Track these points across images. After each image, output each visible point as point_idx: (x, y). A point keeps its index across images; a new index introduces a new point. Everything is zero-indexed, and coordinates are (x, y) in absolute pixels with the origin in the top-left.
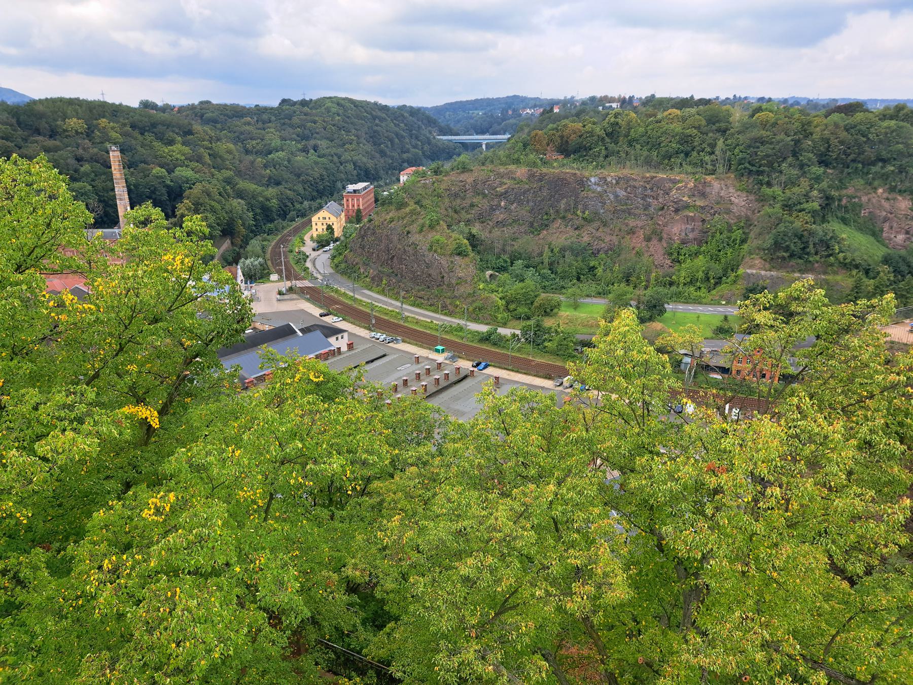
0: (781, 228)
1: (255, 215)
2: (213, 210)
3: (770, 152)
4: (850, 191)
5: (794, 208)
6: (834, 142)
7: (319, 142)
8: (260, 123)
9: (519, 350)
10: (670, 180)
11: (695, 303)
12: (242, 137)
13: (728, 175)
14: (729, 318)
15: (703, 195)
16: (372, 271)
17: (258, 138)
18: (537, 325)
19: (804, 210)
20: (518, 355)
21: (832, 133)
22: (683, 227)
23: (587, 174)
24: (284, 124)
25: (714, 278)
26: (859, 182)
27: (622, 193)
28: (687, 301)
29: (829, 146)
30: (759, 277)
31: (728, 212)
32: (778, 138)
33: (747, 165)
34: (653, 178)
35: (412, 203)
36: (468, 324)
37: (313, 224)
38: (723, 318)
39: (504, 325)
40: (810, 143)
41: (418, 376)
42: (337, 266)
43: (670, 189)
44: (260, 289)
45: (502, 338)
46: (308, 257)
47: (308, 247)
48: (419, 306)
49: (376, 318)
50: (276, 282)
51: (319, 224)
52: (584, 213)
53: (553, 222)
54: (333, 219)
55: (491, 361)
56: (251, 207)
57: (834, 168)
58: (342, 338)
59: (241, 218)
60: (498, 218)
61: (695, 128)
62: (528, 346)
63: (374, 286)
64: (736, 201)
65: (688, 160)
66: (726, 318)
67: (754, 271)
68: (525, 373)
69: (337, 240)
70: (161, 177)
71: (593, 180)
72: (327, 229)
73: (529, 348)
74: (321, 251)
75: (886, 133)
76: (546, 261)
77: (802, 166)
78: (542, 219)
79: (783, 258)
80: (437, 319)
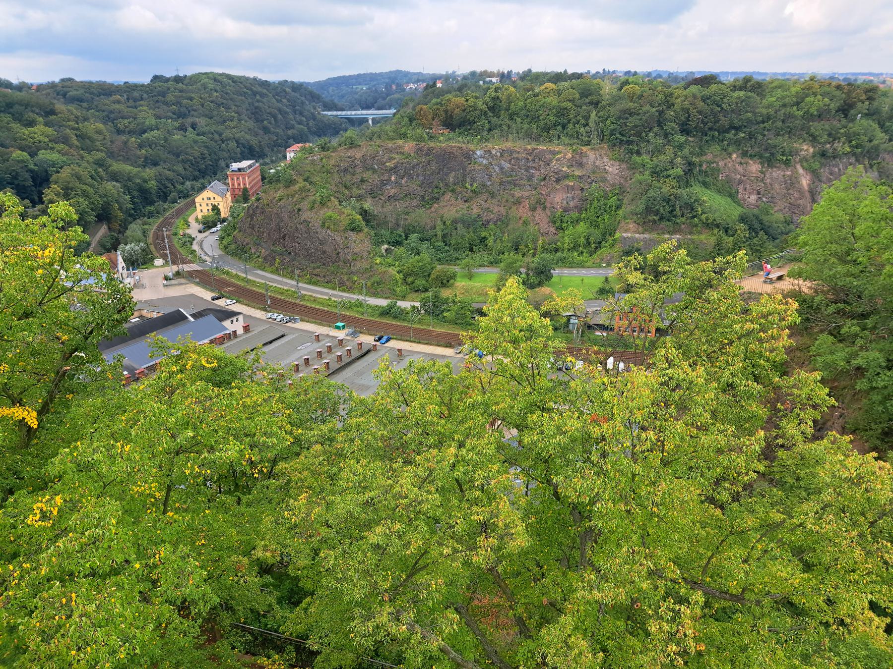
0: (651, 193)
1: (133, 198)
2: (85, 195)
3: (638, 123)
4: (709, 157)
5: (661, 175)
6: (693, 112)
7: (197, 119)
9: (420, 322)
10: (550, 151)
11: (579, 267)
12: (112, 116)
13: (602, 145)
14: (610, 279)
15: (581, 165)
16: (263, 251)
17: (130, 117)
18: (436, 297)
19: (669, 176)
20: (418, 326)
21: (691, 104)
22: (564, 196)
23: (472, 147)
24: (157, 101)
26: (716, 148)
27: (507, 165)
28: (572, 265)
29: (689, 116)
30: (633, 239)
31: (604, 180)
32: (644, 109)
33: (618, 135)
34: (534, 150)
35: (300, 180)
36: (367, 299)
37: (198, 205)
38: (604, 279)
39: (404, 298)
40: (672, 113)
41: (320, 354)
42: (226, 248)
43: (551, 160)
44: (144, 275)
45: (402, 311)
46: (194, 239)
47: (193, 230)
48: (315, 284)
49: (271, 298)
50: (161, 266)
51: (204, 205)
52: (472, 185)
53: (443, 195)
54: (219, 199)
55: (393, 334)
56: (127, 190)
57: (694, 136)
59: (117, 201)
60: (389, 193)
61: (570, 101)
62: (427, 317)
63: (267, 265)
64: (610, 170)
65: (565, 131)
66: (607, 279)
67: (629, 235)
69: (224, 220)
70: (23, 161)
71: (478, 153)
72: (213, 210)
73: (429, 319)
74: (207, 233)
75: (737, 103)
76: (440, 233)
77: (666, 135)
78: (432, 193)
79: (654, 221)
80: (335, 296)
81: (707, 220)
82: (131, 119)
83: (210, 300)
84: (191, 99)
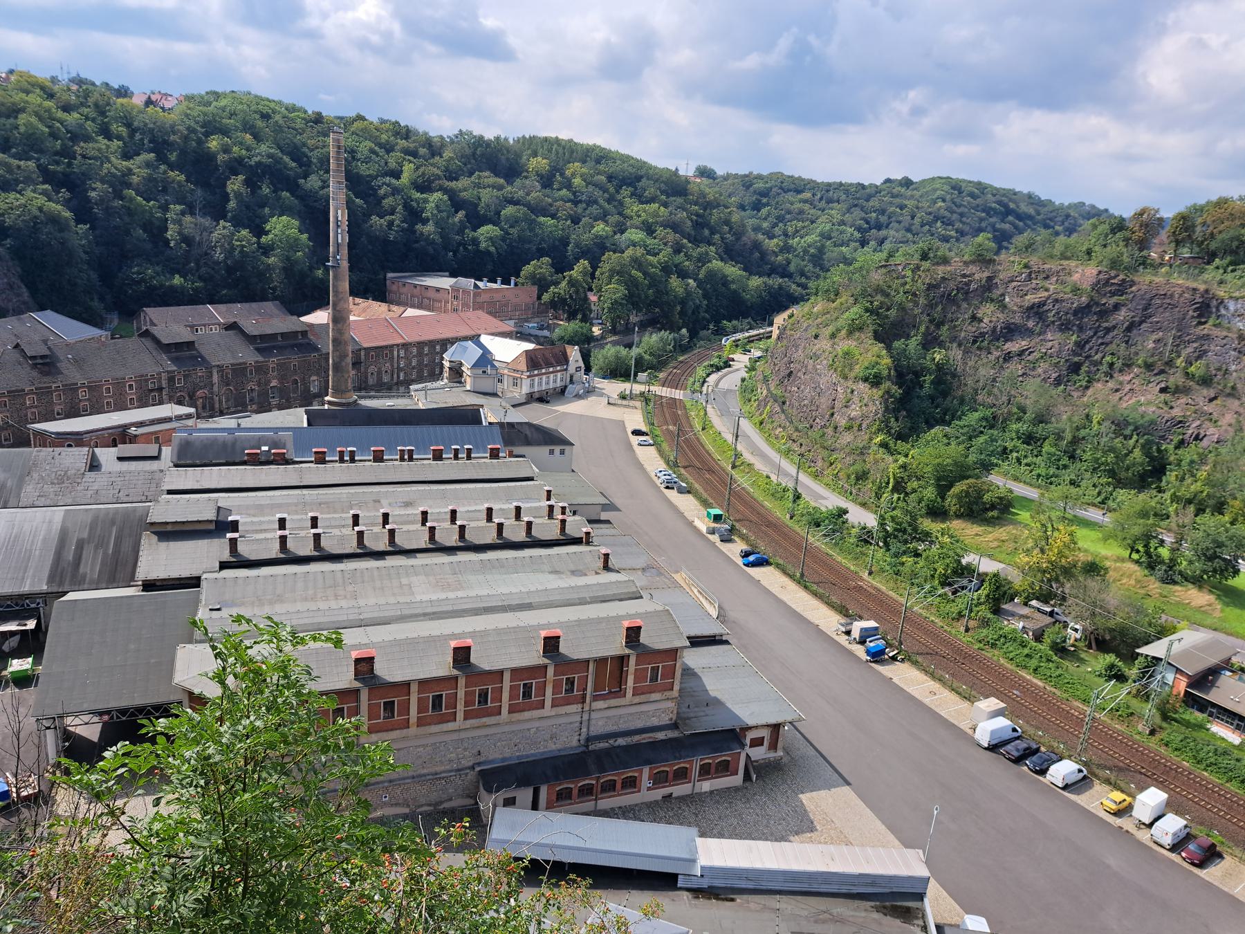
8: (824, 202)
12: (788, 216)
23: (1221, 293)
48: (787, 453)
58: (562, 452)
68: (815, 594)
71: (1232, 306)
76: (1068, 436)
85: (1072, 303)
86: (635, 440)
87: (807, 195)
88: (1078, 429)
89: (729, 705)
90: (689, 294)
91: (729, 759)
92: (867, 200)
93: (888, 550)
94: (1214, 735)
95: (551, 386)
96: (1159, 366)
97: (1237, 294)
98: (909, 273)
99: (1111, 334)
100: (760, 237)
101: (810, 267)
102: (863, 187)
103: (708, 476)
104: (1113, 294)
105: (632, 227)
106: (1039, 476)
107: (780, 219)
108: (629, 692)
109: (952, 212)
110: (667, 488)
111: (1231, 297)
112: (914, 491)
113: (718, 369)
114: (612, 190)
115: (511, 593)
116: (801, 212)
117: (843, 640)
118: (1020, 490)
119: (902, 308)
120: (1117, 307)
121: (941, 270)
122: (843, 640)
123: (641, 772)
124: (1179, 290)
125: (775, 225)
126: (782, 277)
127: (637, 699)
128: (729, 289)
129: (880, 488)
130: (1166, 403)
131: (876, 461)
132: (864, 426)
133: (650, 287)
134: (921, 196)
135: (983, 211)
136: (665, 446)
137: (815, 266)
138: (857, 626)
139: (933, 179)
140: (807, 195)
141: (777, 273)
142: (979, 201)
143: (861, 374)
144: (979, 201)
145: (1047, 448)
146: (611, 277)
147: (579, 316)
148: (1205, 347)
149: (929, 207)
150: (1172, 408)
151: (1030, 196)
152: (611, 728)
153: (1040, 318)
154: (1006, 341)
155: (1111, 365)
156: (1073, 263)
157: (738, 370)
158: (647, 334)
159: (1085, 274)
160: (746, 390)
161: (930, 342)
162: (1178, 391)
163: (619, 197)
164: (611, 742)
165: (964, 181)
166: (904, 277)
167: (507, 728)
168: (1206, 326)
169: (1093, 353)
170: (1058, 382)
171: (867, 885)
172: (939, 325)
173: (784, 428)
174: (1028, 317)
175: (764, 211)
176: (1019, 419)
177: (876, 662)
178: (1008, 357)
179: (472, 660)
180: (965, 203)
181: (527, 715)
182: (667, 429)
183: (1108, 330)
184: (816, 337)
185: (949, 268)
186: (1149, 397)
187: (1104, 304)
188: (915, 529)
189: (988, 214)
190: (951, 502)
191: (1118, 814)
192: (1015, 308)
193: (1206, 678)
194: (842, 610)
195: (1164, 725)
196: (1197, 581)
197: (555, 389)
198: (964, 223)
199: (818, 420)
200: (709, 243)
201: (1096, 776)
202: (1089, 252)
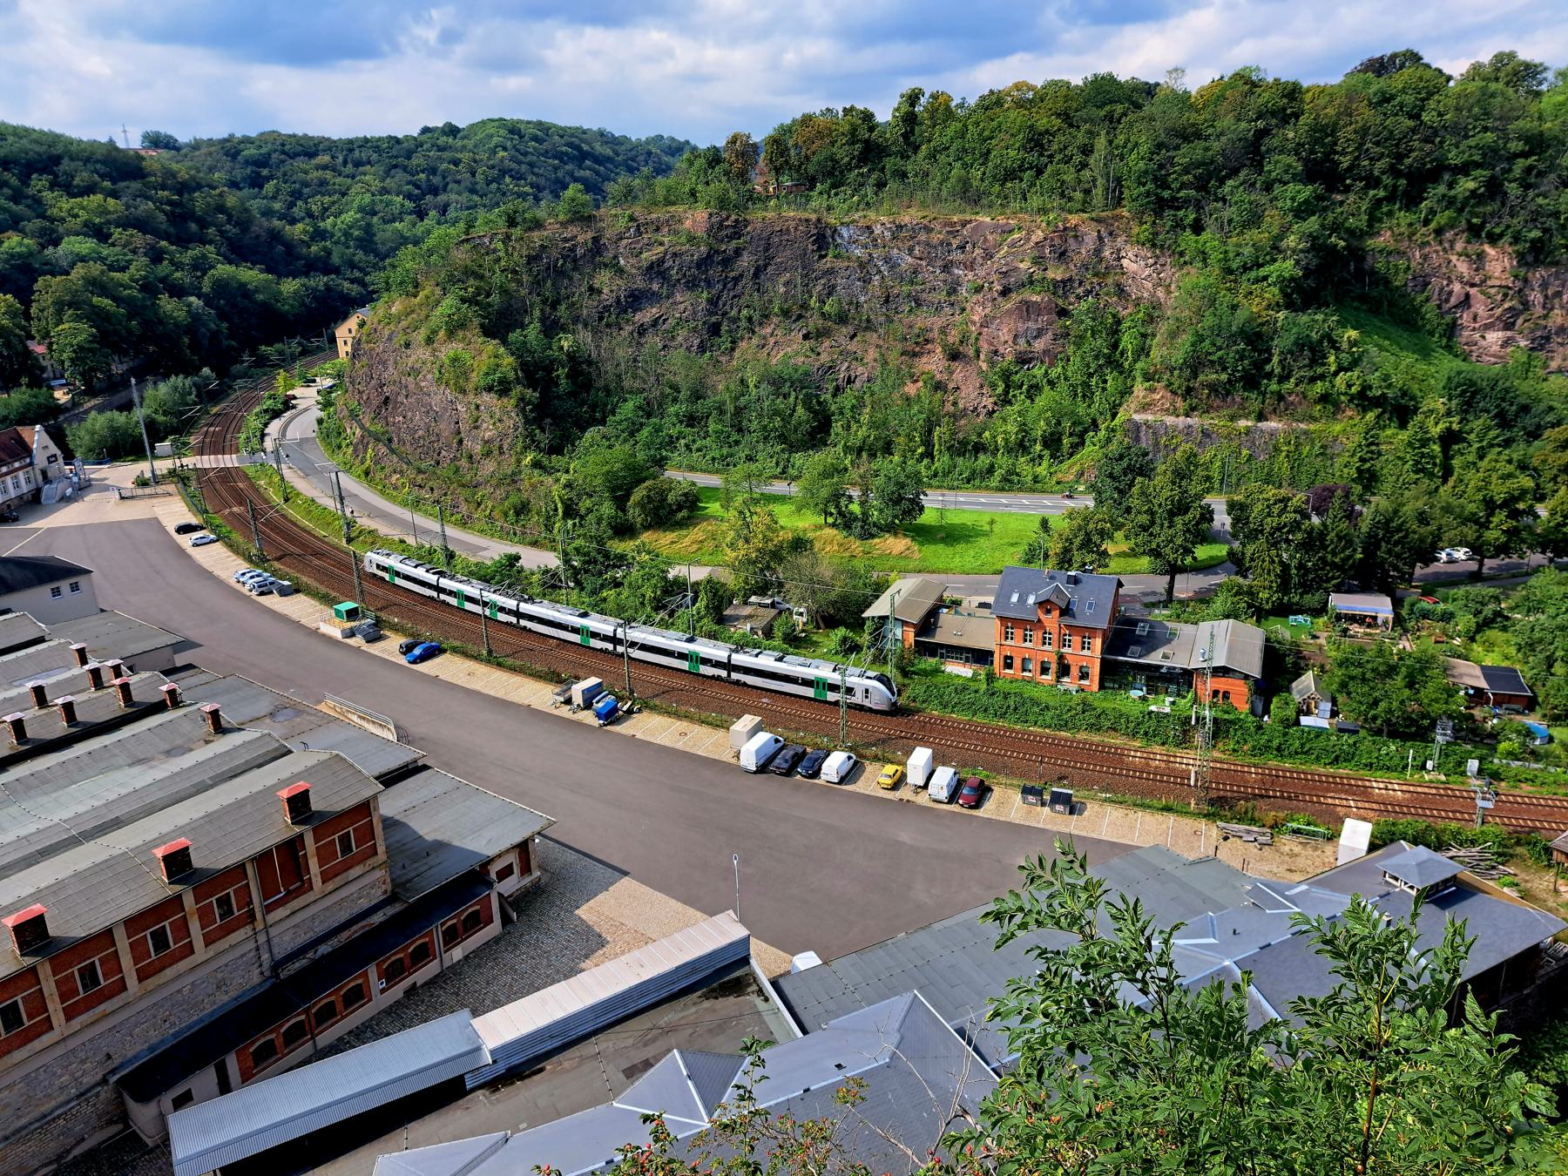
3: (1199, 154)
4: (1383, 240)
6: (1346, 133)
8: (350, 165)
10: (997, 226)
11: (1020, 490)
12: (306, 191)
13: (1119, 211)
15: (1062, 256)
19: (1265, 278)
22: (1021, 327)
25: (1071, 435)
26: (1403, 218)
28: (1010, 483)
31: (1121, 291)
33: (1150, 186)
34: (964, 224)
38: (1036, 525)
48: (416, 504)
58: (75, 587)
61: (1058, 115)
67: (1150, 418)
68: (513, 669)
75: (1458, 109)
76: (730, 407)
79: (1213, 388)
81: (1349, 386)
82: (336, 197)
83: (171, 530)
84: (456, 163)
85: (692, 255)
86: (186, 541)
87: (324, 159)
88: (737, 399)
89: (456, 843)
90: (195, 317)
91: (477, 907)
92: (409, 158)
93: (582, 589)
94: (949, 674)
95: (13, 493)
96: (796, 311)
97: (846, 220)
98: (500, 245)
99: (741, 284)
100: (277, 223)
101: (360, 255)
102: (398, 141)
103: (317, 562)
104: (731, 238)
105: (69, 233)
106: (713, 459)
107: (297, 195)
108: (317, 881)
109: (519, 163)
110: (262, 594)
111: (842, 224)
112: (589, 511)
113: (276, 414)
114: (14, 181)
115: (78, 815)
116: (323, 182)
117: (565, 712)
118: (703, 480)
119: (504, 291)
120: (738, 252)
121: (536, 234)
122: (565, 712)
123: (365, 974)
124: (793, 224)
125: (292, 205)
126: (327, 272)
127: (330, 886)
128: (255, 302)
129: (548, 518)
130: (812, 350)
131: (534, 487)
132: (505, 447)
133: (130, 317)
134: (475, 146)
135: (555, 157)
136: (236, 537)
137: (366, 253)
138: (577, 691)
139: (483, 122)
140: (325, 159)
141: (317, 270)
142: (545, 146)
143: (482, 383)
144: (545, 146)
145: (712, 427)
146: (59, 313)
147: (24, 380)
148: (833, 281)
149: (489, 159)
150: (819, 354)
151: (602, 134)
152: (302, 939)
153: (664, 278)
154: (635, 311)
155: (750, 319)
156: (681, 209)
157: (306, 410)
158: (150, 385)
159: (696, 219)
160: (330, 434)
161: (551, 328)
162: (821, 334)
163: (30, 191)
164: (310, 955)
165: (520, 121)
166: (495, 251)
167: (143, 1005)
168: (828, 258)
169: (727, 307)
170: (702, 349)
171: (687, 976)
172: (554, 305)
173: (401, 472)
174: (651, 279)
175: (269, 187)
176: (675, 400)
177: (609, 724)
178: (642, 330)
179: (51, 932)
180: (531, 150)
181: (169, 973)
182: (232, 514)
183: (736, 280)
184: (407, 345)
185: (545, 233)
186: (795, 347)
187: (725, 251)
188: (607, 556)
189: (561, 161)
190: (634, 514)
191: (895, 786)
192: (634, 271)
193: (928, 624)
194: (553, 677)
195: (907, 681)
196: (891, 529)
197: (20, 497)
198: (537, 175)
199: (444, 453)
200: (204, 241)
201: (864, 757)
202: (693, 193)
